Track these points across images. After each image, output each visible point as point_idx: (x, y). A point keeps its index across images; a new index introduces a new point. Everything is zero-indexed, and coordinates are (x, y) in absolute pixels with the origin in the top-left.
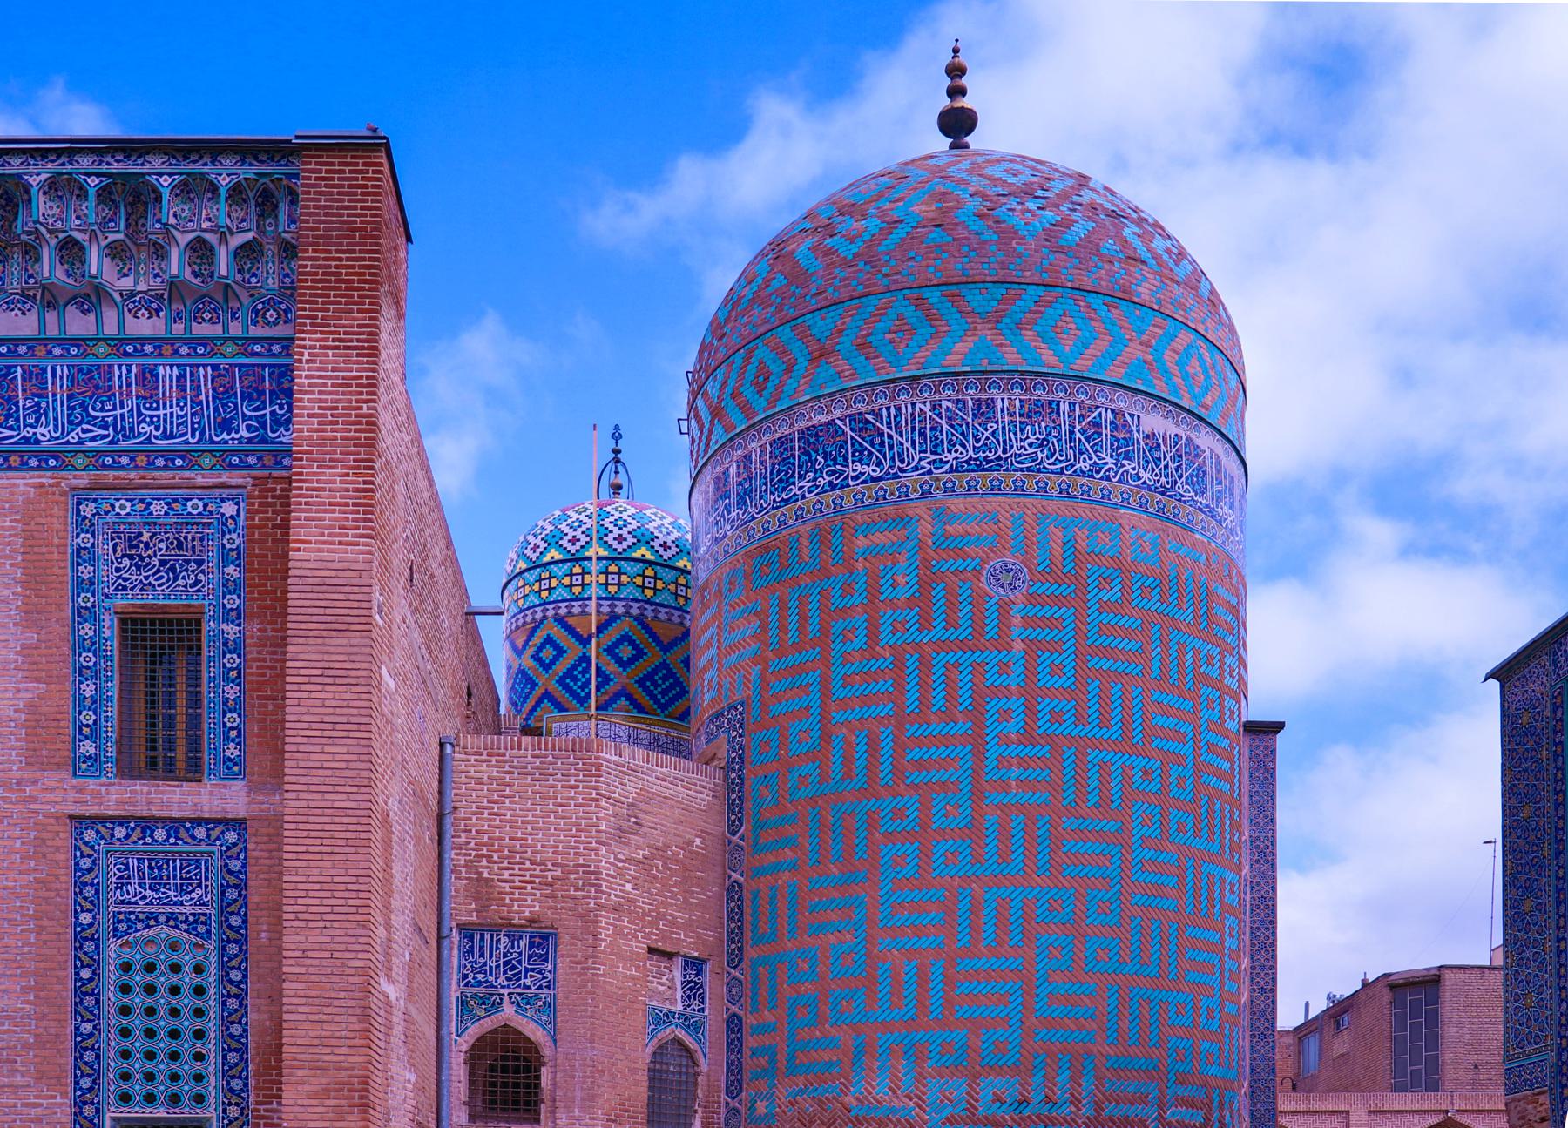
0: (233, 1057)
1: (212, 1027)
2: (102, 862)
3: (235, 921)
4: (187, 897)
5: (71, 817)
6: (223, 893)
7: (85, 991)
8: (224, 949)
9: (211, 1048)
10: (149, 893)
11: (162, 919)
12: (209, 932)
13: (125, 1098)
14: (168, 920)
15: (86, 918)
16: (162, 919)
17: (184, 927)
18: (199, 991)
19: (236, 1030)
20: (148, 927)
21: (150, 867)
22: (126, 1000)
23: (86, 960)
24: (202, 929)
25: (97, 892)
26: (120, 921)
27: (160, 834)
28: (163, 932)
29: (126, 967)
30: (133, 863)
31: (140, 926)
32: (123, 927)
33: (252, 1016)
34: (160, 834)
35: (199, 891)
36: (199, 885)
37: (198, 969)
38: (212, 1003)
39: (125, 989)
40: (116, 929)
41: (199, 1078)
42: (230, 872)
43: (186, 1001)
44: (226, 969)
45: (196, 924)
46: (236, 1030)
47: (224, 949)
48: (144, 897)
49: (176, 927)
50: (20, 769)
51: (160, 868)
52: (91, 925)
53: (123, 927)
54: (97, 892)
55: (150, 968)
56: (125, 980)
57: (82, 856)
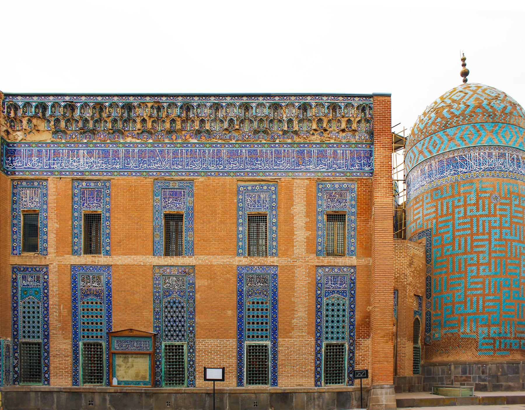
0: (351, 327)
1: (347, 319)
2: (323, 277)
3: (353, 292)
4: (342, 286)
5: (316, 266)
6: (350, 285)
7: (318, 311)
8: (350, 299)
9: (347, 324)
10: (333, 285)
11: (336, 292)
12: (346, 295)
13: (327, 338)
14: (337, 292)
15: (319, 292)
16: (336, 292)
17: (341, 294)
18: (344, 310)
19: (352, 320)
20: (333, 294)
21: (334, 279)
22: (327, 313)
23: (319, 303)
24: (345, 294)
25: (322, 285)
26: (326, 293)
27: (336, 270)
28: (336, 295)
29: (327, 305)
30: (329, 278)
31: (331, 294)
32: (327, 294)
33: (356, 316)
34: (336, 270)
35: (344, 284)
36: (344, 283)
37: (343, 305)
38: (347, 313)
39: (327, 310)
40: (325, 295)
41: (343, 333)
42: (352, 280)
43: (341, 313)
44: (350, 304)
45: (343, 293)
46: (352, 320)
47: (350, 299)
48: (332, 286)
49: (339, 294)
50: (305, 254)
51: (336, 279)
52: (320, 294)
53: (327, 294)
54: (322, 285)
55: (333, 305)
56: (327, 308)
57: (318, 276)
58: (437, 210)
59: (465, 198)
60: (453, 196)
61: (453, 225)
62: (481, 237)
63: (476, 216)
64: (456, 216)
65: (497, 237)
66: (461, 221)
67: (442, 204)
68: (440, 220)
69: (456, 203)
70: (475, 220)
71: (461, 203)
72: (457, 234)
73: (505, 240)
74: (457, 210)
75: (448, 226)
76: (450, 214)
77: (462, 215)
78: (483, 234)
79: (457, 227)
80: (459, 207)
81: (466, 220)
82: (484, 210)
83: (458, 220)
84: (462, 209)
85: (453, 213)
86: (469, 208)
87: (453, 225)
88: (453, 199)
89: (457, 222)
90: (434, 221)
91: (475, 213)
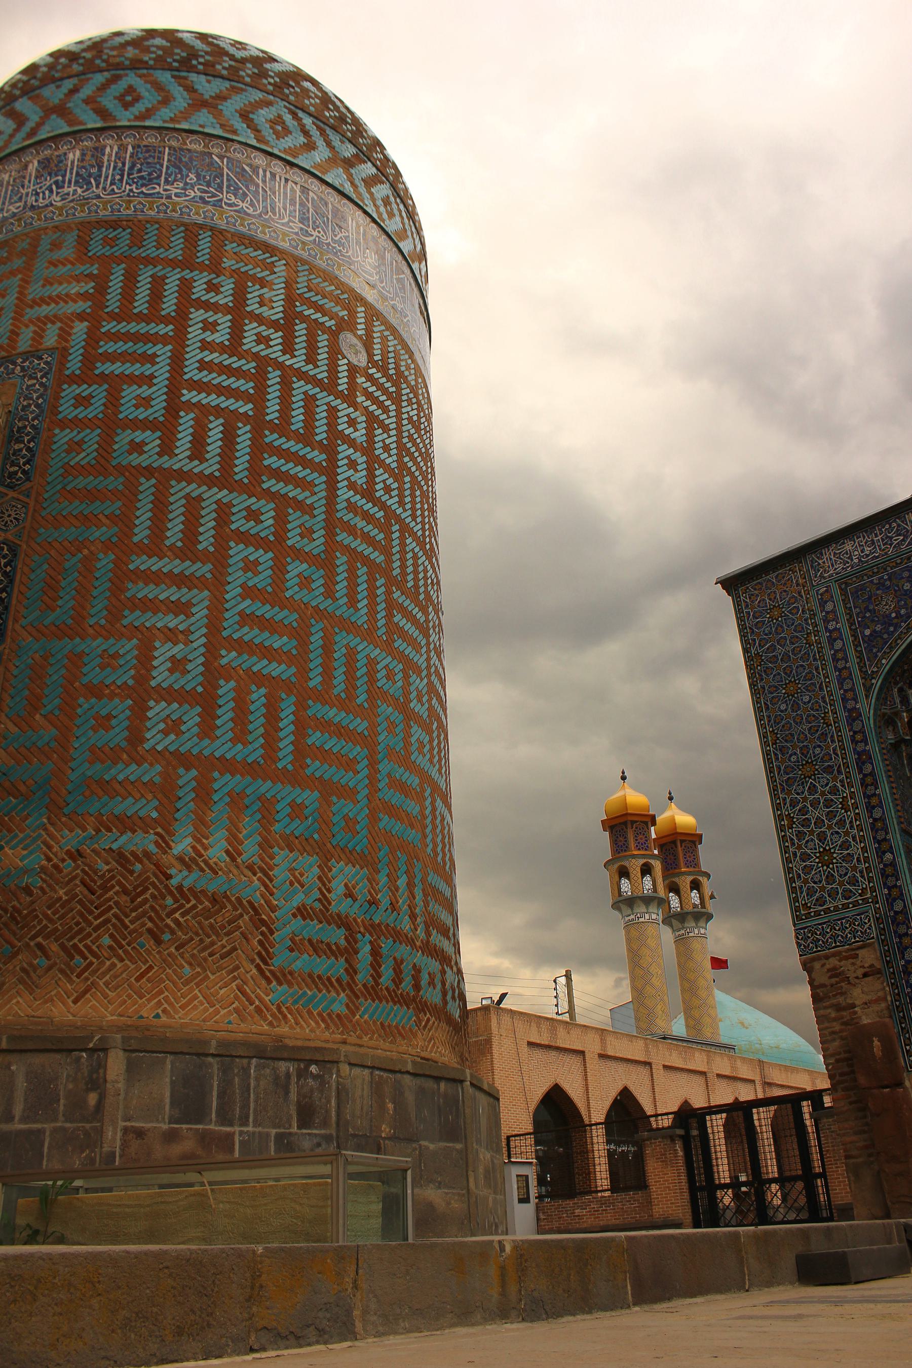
58: (102, 289)
59: (240, 295)
60: (188, 263)
61: (177, 362)
62: (292, 446)
63: (280, 366)
64: (195, 333)
65: (360, 478)
66: (214, 357)
67: (130, 280)
68: (108, 326)
69: (199, 290)
70: (274, 377)
71: (225, 298)
72: (187, 395)
73: (383, 506)
74: (198, 315)
75: (151, 359)
76: (166, 320)
77: (221, 336)
78: (306, 438)
79: (191, 372)
80: (207, 306)
81: (235, 363)
82: (311, 359)
83: (202, 349)
84: (224, 321)
85: (181, 320)
86: (251, 329)
87: (177, 362)
88: (187, 274)
89: (193, 355)
90: (80, 329)
91: (275, 352)
